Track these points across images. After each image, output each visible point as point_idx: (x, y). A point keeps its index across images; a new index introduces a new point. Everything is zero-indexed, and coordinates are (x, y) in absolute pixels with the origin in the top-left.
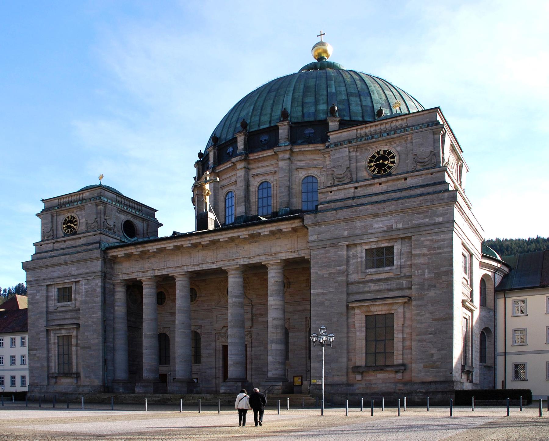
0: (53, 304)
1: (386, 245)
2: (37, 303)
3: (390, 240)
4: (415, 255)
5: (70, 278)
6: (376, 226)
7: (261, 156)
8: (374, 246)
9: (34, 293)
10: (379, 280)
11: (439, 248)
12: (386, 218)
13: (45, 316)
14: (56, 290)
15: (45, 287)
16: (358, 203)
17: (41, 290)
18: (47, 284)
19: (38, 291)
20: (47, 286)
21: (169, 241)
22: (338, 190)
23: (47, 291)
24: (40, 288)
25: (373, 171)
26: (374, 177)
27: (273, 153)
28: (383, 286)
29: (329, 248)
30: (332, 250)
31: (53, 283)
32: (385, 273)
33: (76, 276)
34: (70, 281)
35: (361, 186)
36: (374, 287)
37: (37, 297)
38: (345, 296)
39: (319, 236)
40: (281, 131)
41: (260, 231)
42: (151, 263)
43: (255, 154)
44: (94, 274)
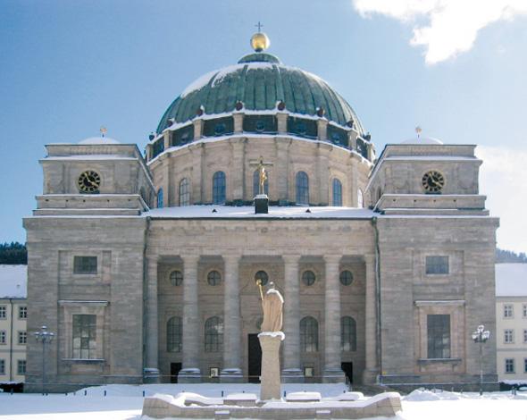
0: (67, 274)
1: (442, 254)
2: (43, 271)
4: (469, 267)
8: (433, 254)
9: (39, 259)
10: (438, 285)
11: (484, 263)
12: (444, 232)
13: (56, 288)
14: (72, 258)
15: (57, 253)
17: (51, 256)
18: (61, 249)
19: (46, 258)
20: (60, 252)
23: (60, 258)
24: (48, 254)
26: (427, 193)
32: (442, 279)
33: (107, 245)
38: (410, 296)
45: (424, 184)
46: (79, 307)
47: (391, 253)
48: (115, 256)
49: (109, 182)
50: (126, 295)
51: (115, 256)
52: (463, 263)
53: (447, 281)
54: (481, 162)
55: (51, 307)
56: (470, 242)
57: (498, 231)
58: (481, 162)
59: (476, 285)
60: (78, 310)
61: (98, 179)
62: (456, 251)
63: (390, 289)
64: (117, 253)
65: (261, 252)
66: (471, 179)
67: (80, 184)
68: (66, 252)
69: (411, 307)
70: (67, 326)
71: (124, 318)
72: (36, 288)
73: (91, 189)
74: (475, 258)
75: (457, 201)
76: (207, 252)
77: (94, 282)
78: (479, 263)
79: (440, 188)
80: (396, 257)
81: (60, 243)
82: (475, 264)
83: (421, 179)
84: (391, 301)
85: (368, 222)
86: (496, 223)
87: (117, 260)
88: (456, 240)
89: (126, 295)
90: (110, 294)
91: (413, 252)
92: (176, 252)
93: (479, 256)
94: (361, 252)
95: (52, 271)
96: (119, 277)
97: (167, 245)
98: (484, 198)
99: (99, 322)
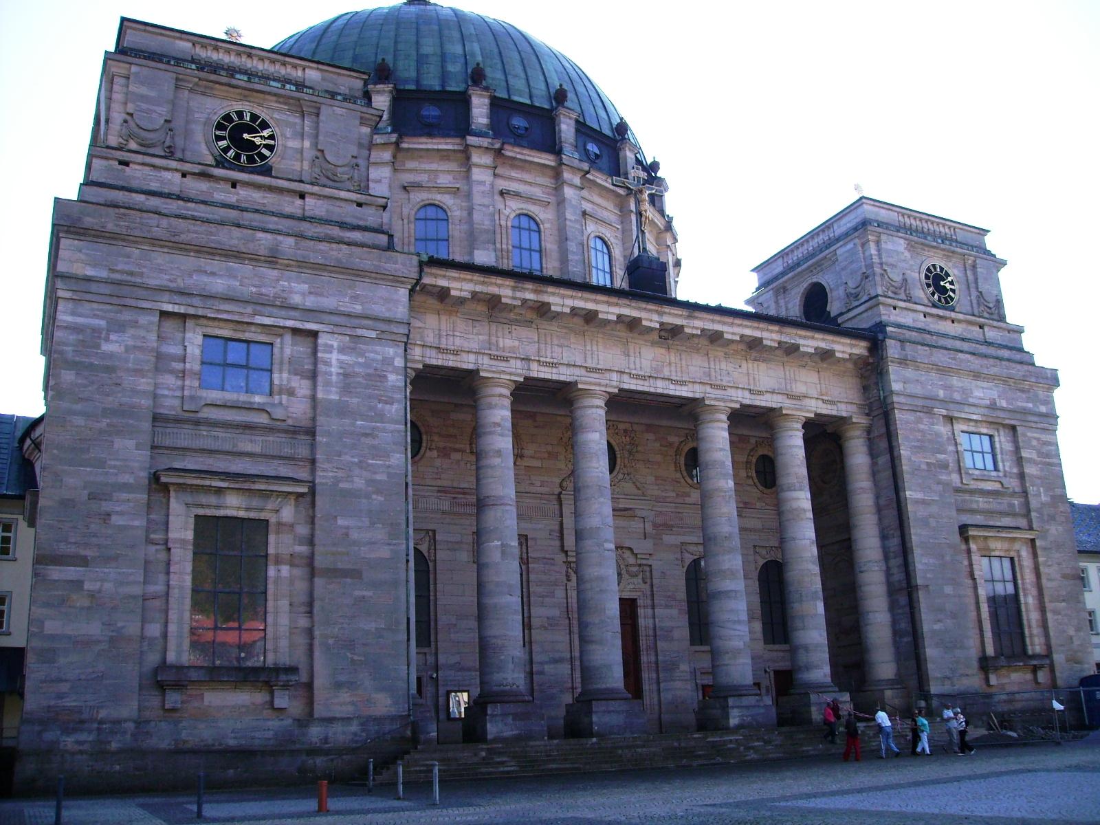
2: (110, 370)
3: (991, 423)
4: (1030, 460)
5: (283, 313)
6: (978, 393)
9: (96, 331)
12: (985, 385)
16: (939, 344)
17: (135, 324)
18: (169, 308)
19: (120, 327)
20: (164, 314)
21: (614, 300)
22: (906, 309)
24: (126, 316)
25: (933, 294)
26: (934, 306)
27: (553, 164)
28: (992, 504)
29: (921, 414)
31: (200, 312)
34: (282, 323)
35: (932, 315)
36: (981, 502)
39: (906, 386)
40: (564, 127)
41: (801, 342)
42: (519, 339)
43: (517, 150)
45: (929, 286)
46: (219, 491)
47: (910, 417)
48: (329, 349)
49: (301, 151)
50: (360, 465)
51: (329, 349)
52: (1017, 449)
53: (997, 486)
54: (1003, 263)
55: (125, 487)
56: (1025, 412)
57: (1058, 394)
58: (1003, 263)
59: (1044, 498)
60: (213, 500)
62: (1004, 426)
63: (919, 496)
65: (660, 387)
67: (219, 138)
68: (184, 317)
69: (956, 538)
71: (354, 535)
72: (79, 421)
73: (251, 160)
74: (1034, 443)
75: (986, 329)
76: (541, 372)
77: (263, 419)
78: (1040, 454)
79: (952, 299)
80: (922, 427)
81: (161, 290)
82: (1034, 456)
83: (923, 276)
84: (925, 522)
85: (864, 344)
86: (1051, 380)
87: (334, 356)
88: (1004, 404)
89: (360, 465)
90: (313, 462)
91: (944, 416)
93: (1038, 439)
94: (843, 410)
95: (139, 372)
96: (342, 410)
97: (460, 343)
98: (1019, 331)
99: (276, 544)
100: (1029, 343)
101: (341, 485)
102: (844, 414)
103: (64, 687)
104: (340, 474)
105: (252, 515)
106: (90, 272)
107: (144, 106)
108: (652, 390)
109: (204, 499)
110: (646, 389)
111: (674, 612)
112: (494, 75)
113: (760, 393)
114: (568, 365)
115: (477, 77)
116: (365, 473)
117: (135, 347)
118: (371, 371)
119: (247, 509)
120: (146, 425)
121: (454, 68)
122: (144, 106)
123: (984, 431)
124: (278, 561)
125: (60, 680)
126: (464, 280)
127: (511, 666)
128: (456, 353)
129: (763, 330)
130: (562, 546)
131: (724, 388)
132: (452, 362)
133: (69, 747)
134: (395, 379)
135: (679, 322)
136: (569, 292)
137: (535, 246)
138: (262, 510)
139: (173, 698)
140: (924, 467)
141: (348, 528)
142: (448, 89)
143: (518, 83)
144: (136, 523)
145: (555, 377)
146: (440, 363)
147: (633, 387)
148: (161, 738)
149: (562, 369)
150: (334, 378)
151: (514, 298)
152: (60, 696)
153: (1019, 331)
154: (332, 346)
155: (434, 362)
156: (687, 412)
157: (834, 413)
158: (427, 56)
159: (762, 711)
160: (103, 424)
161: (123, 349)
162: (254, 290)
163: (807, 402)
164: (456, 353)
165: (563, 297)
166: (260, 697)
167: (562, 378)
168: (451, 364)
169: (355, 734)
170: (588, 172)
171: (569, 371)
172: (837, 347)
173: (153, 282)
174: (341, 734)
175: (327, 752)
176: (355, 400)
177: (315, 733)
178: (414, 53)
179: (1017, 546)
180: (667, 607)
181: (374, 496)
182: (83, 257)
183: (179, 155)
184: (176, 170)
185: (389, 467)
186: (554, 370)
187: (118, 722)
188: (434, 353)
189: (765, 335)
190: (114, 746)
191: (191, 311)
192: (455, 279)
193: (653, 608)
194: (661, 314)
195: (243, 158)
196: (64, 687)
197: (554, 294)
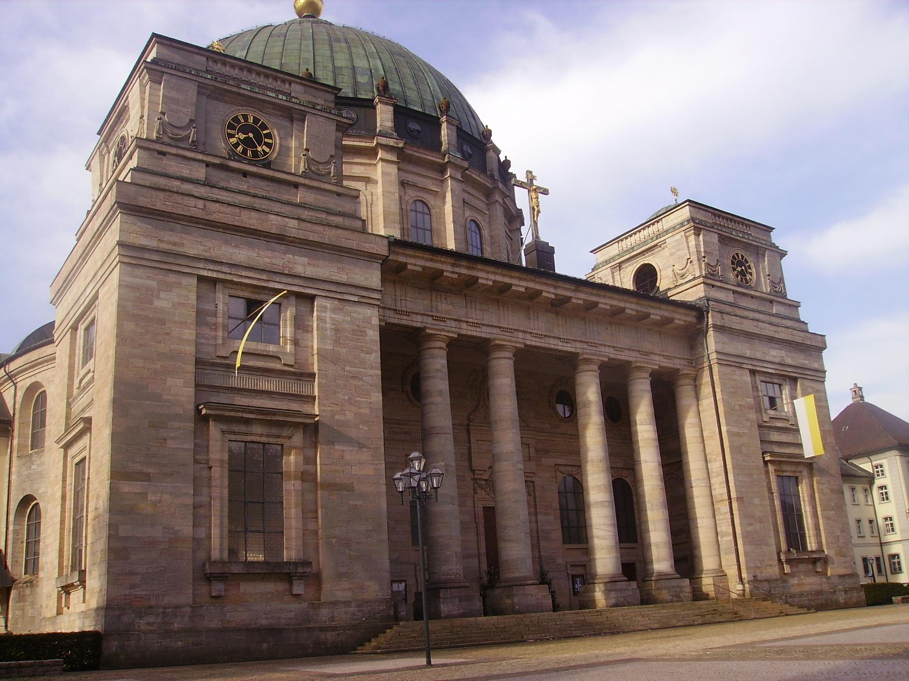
2: (162, 322)
5: (290, 280)
7: (422, 156)
19: (169, 287)
20: (201, 279)
21: (524, 276)
24: (172, 278)
26: (739, 285)
30: (738, 371)
37: (157, 303)
42: (452, 304)
44: (364, 293)
48: (323, 309)
58: (783, 254)
60: (242, 428)
61: (269, 136)
64: (328, 304)
65: (552, 344)
66: (780, 276)
70: (216, 472)
71: (348, 457)
76: (467, 330)
80: (736, 377)
85: (694, 313)
92: (417, 321)
94: (677, 364)
98: (795, 306)
100: (804, 314)
101: (336, 417)
102: (678, 367)
103: (136, 580)
104: (336, 408)
105: (272, 440)
106: (143, 241)
107: (174, 107)
108: (547, 346)
109: (236, 428)
110: (542, 345)
111: (551, 518)
112: (394, 87)
113: (621, 349)
114: (488, 326)
115: (384, 89)
116: (354, 409)
117: (179, 303)
118: (355, 327)
119: (268, 436)
120: (191, 368)
121: (362, 79)
122: (174, 107)
123: (776, 381)
124: (289, 479)
125: (132, 574)
126: (418, 257)
127: (455, 559)
128: (408, 314)
129: (625, 301)
130: (471, 466)
131: (595, 345)
132: (405, 321)
133: (143, 628)
134: (373, 335)
135: (568, 294)
136: (492, 269)
137: (428, 226)
138: (278, 437)
139: (218, 588)
140: (737, 408)
141: (343, 451)
142: (359, 96)
143: (412, 95)
144: (187, 446)
145: (478, 334)
146: (396, 321)
147: (533, 343)
148: (212, 620)
149: (484, 329)
150: (328, 333)
151: (453, 272)
152: (133, 586)
153: (795, 306)
154: (326, 307)
155: (392, 321)
156: (570, 363)
157: (671, 366)
158: (341, 68)
159: (631, 593)
160: (158, 365)
161: (170, 305)
162: (268, 260)
163: (653, 357)
164: (408, 314)
165: (488, 272)
166: (281, 586)
167: (484, 335)
168: (404, 322)
169: (354, 614)
170: (467, 169)
171: (488, 330)
172: (676, 316)
173: (192, 252)
174: (343, 615)
175: (335, 629)
176: (344, 351)
177: (325, 613)
178: (330, 66)
179: (801, 468)
180: (546, 514)
181: (361, 427)
182: (138, 229)
183: (201, 148)
184: (202, 161)
185: (370, 403)
186: (478, 329)
187: (177, 607)
188: (392, 314)
189: (628, 305)
190: (176, 626)
191: (222, 276)
192: (411, 256)
193: (536, 515)
194: (556, 287)
195: (249, 153)
196: (136, 580)
197: (481, 270)
